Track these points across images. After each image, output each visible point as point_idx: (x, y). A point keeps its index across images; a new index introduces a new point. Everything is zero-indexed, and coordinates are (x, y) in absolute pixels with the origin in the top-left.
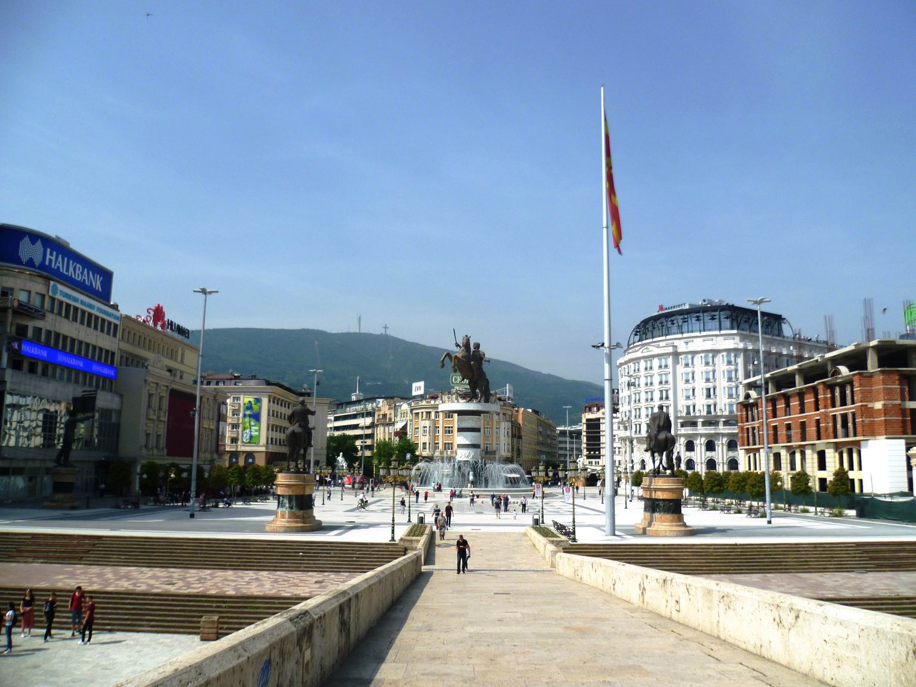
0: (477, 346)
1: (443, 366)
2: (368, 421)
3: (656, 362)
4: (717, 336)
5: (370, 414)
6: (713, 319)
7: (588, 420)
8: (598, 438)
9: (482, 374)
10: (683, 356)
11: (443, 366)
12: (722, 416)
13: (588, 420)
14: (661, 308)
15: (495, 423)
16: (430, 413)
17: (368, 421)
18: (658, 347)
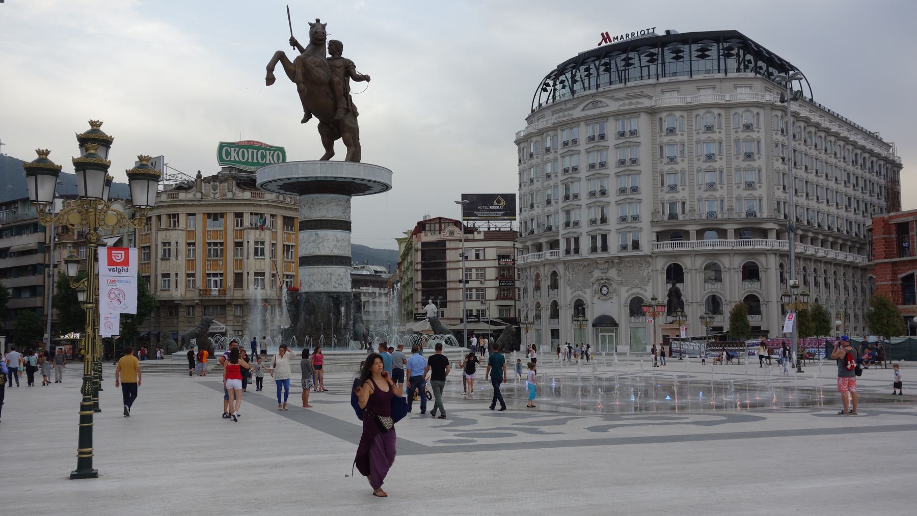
0: (337, 47)
1: (270, 80)
2: (28, 240)
3: (612, 128)
4: (721, 80)
5: (34, 227)
6: (703, 56)
7: (424, 244)
8: (443, 274)
9: (352, 112)
10: (664, 115)
11: (270, 80)
12: (729, 221)
13: (424, 244)
14: (606, 37)
16: (175, 216)
17: (28, 240)
18: (618, 100)
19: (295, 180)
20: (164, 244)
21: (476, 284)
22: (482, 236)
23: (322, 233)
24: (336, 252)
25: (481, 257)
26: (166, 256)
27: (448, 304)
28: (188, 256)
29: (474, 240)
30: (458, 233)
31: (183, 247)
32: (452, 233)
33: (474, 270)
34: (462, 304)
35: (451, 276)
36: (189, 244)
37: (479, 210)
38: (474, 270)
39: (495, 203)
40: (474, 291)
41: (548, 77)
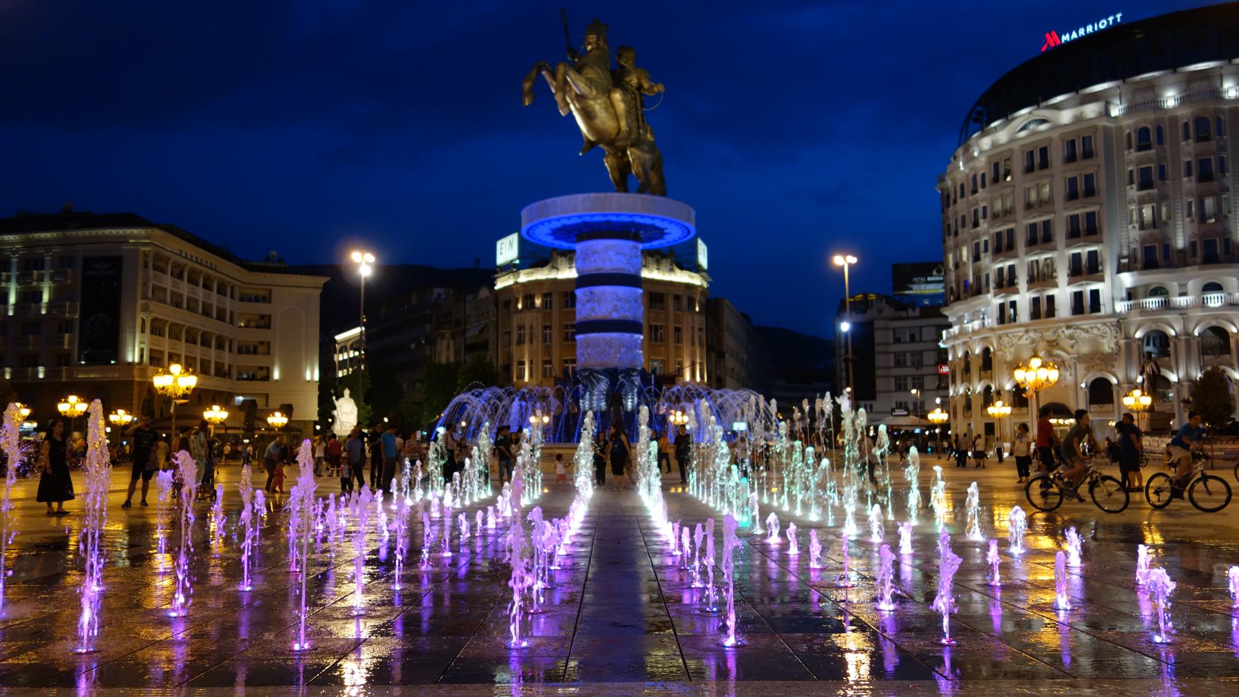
15: (671, 316)
19: (556, 225)
20: (521, 328)
21: (913, 371)
22: (917, 312)
23: (598, 290)
24: (615, 316)
25: (917, 338)
26: (520, 342)
27: (878, 395)
28: (545, 340)
29: (907, 318)
30: (888, 311)
31: (538, 332)
32: (880, 311)
33: (908, 355)
34: (894, 395)
35: (879, 360)
36: (545, 328)
37: (914, 283)
38: (908, 355)
39: (934, 273)
40: (909, 381)
41: (979, 103)
